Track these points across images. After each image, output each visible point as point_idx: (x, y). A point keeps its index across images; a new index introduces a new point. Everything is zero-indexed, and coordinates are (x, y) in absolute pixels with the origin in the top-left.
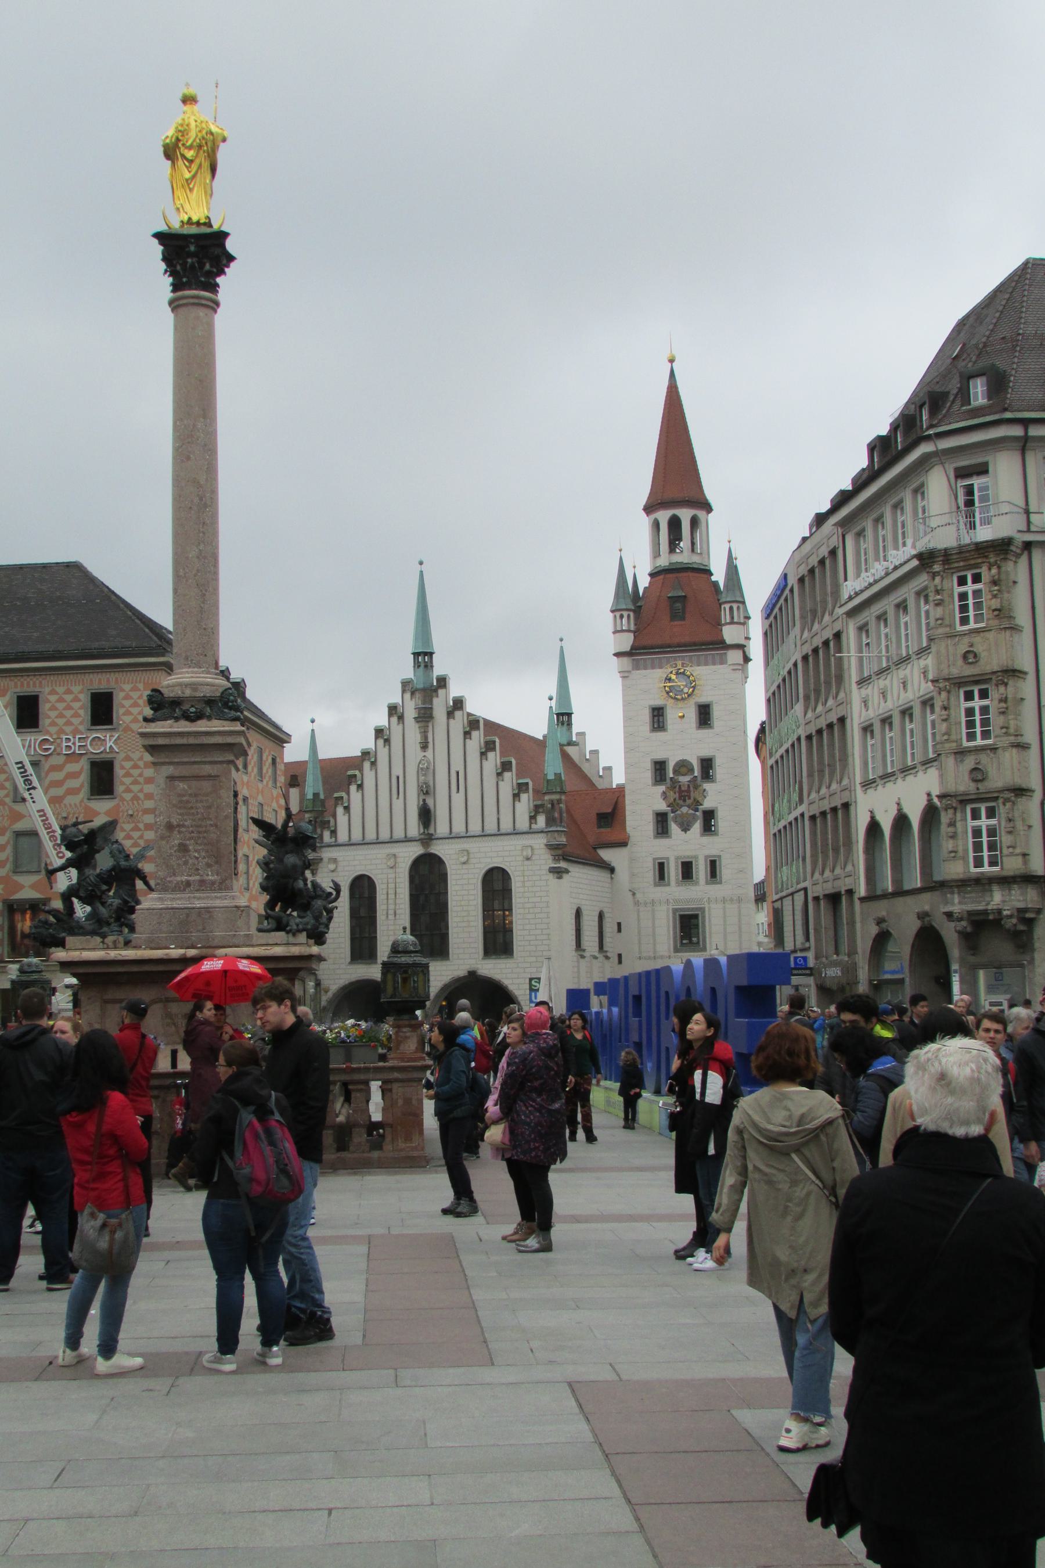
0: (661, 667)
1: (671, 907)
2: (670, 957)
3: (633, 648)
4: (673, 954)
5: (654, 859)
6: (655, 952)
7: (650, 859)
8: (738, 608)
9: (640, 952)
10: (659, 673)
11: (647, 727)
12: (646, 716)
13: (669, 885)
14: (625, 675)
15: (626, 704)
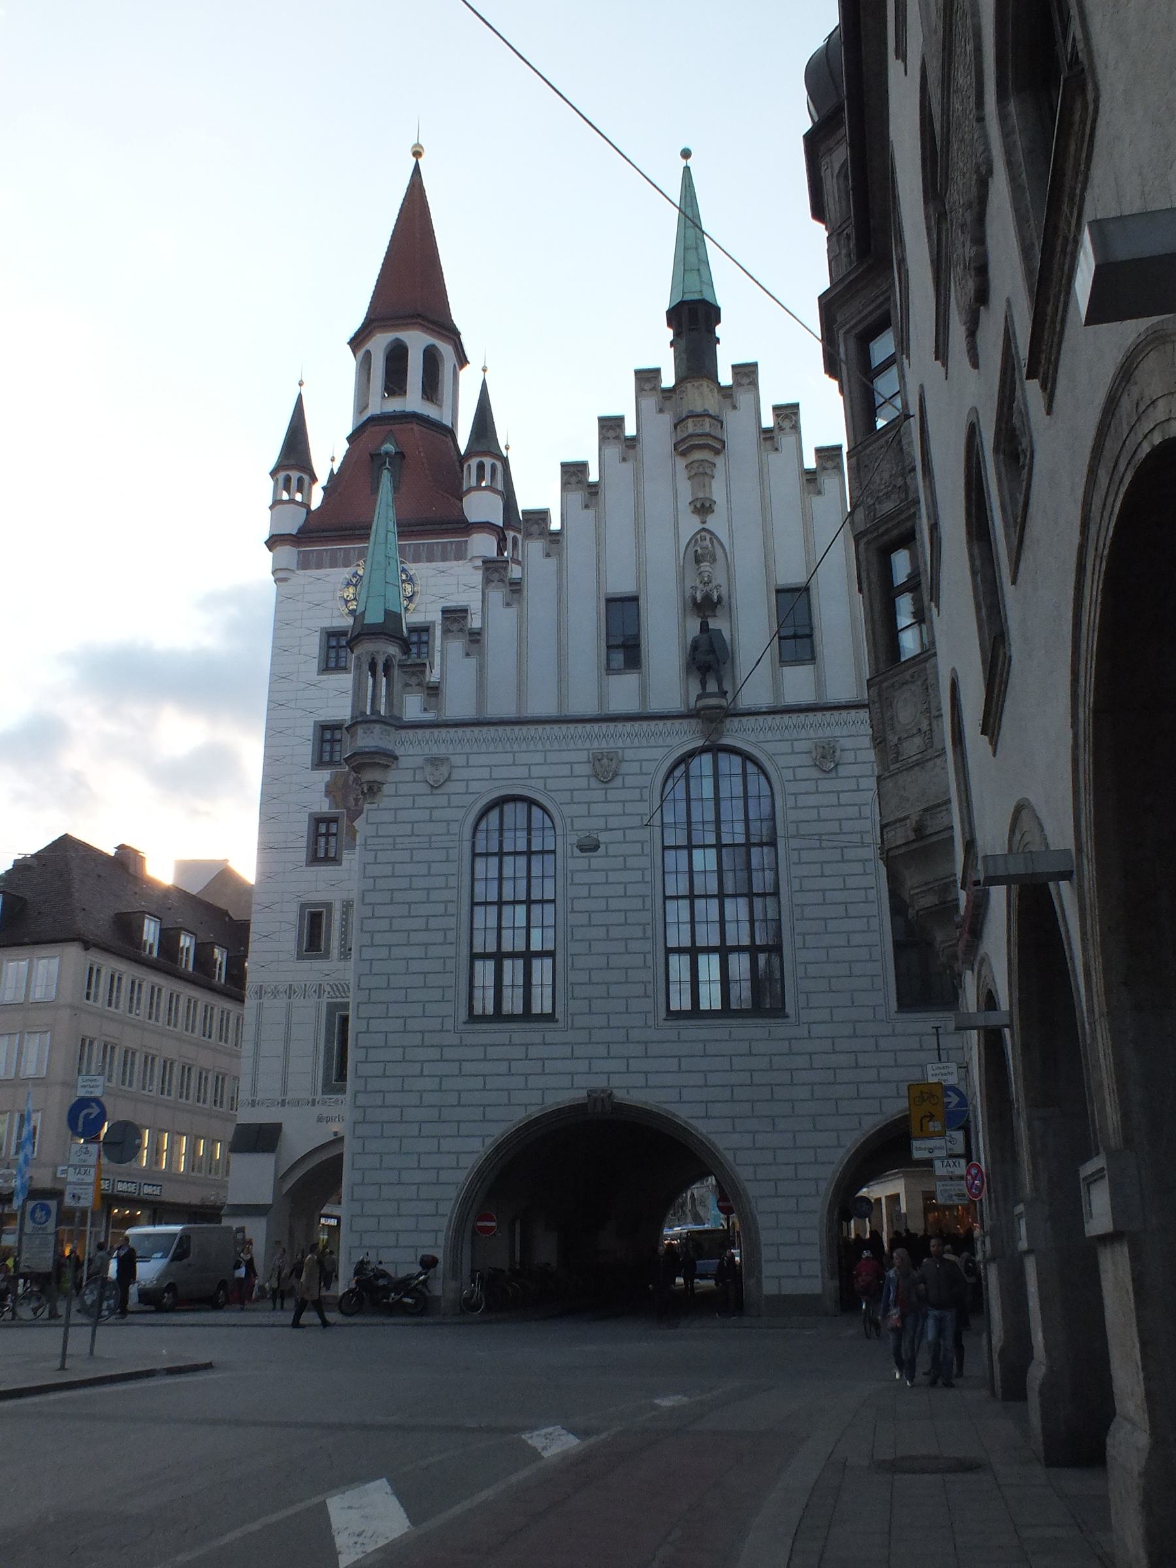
0: (346, 565)
1: (325, 1000)
2: (314, 1103)
3: (300, 531)
4: (319, 1096)
5: (303, 906)
6: (284, 1093)
7: (295, 908)
8: (493, 467)
9: (254, 1093)
10: (345, 573)
11: (314, 665)
12: (313, 645)
13: (326, 956)
14: (280, 574)
15: (282, 623)
